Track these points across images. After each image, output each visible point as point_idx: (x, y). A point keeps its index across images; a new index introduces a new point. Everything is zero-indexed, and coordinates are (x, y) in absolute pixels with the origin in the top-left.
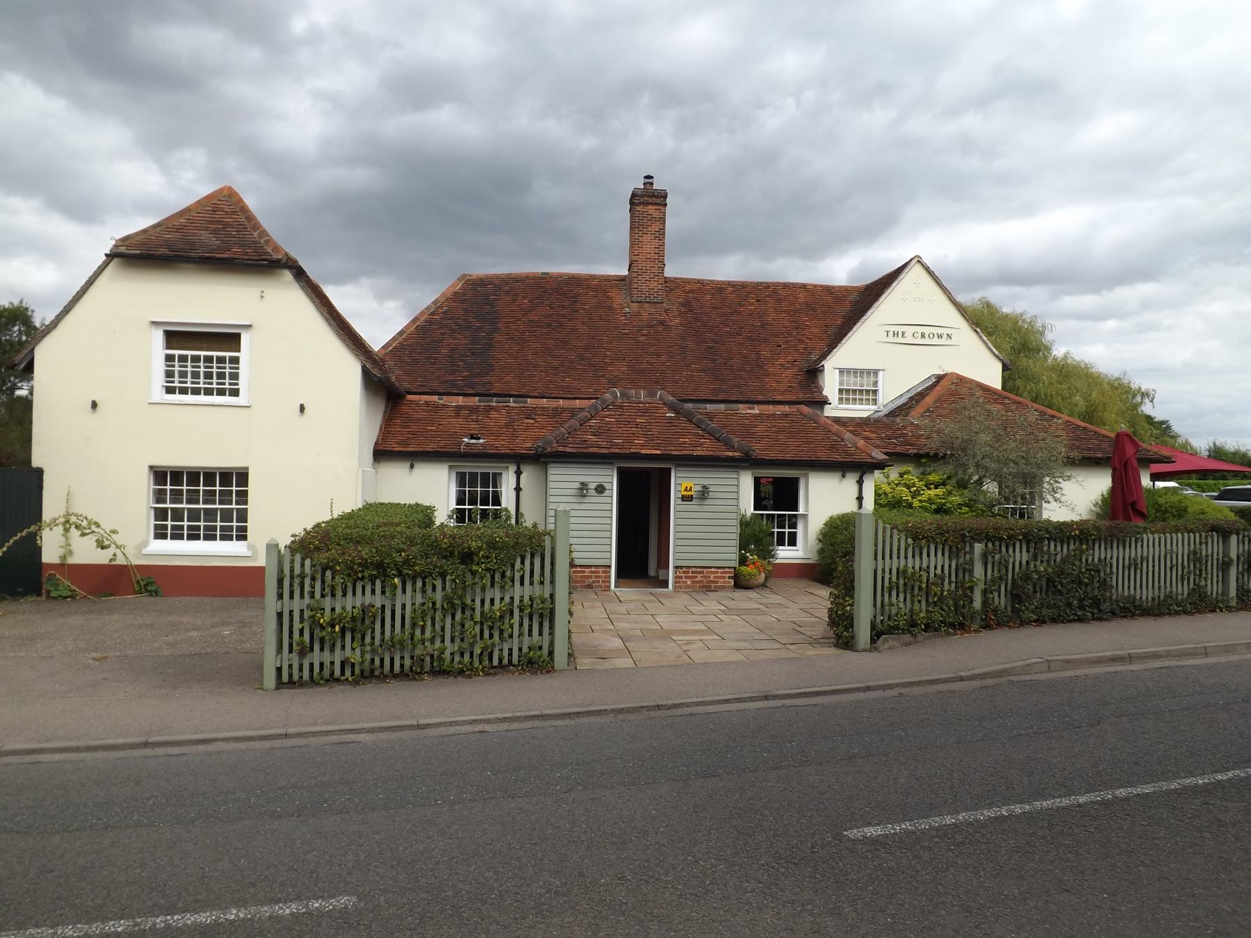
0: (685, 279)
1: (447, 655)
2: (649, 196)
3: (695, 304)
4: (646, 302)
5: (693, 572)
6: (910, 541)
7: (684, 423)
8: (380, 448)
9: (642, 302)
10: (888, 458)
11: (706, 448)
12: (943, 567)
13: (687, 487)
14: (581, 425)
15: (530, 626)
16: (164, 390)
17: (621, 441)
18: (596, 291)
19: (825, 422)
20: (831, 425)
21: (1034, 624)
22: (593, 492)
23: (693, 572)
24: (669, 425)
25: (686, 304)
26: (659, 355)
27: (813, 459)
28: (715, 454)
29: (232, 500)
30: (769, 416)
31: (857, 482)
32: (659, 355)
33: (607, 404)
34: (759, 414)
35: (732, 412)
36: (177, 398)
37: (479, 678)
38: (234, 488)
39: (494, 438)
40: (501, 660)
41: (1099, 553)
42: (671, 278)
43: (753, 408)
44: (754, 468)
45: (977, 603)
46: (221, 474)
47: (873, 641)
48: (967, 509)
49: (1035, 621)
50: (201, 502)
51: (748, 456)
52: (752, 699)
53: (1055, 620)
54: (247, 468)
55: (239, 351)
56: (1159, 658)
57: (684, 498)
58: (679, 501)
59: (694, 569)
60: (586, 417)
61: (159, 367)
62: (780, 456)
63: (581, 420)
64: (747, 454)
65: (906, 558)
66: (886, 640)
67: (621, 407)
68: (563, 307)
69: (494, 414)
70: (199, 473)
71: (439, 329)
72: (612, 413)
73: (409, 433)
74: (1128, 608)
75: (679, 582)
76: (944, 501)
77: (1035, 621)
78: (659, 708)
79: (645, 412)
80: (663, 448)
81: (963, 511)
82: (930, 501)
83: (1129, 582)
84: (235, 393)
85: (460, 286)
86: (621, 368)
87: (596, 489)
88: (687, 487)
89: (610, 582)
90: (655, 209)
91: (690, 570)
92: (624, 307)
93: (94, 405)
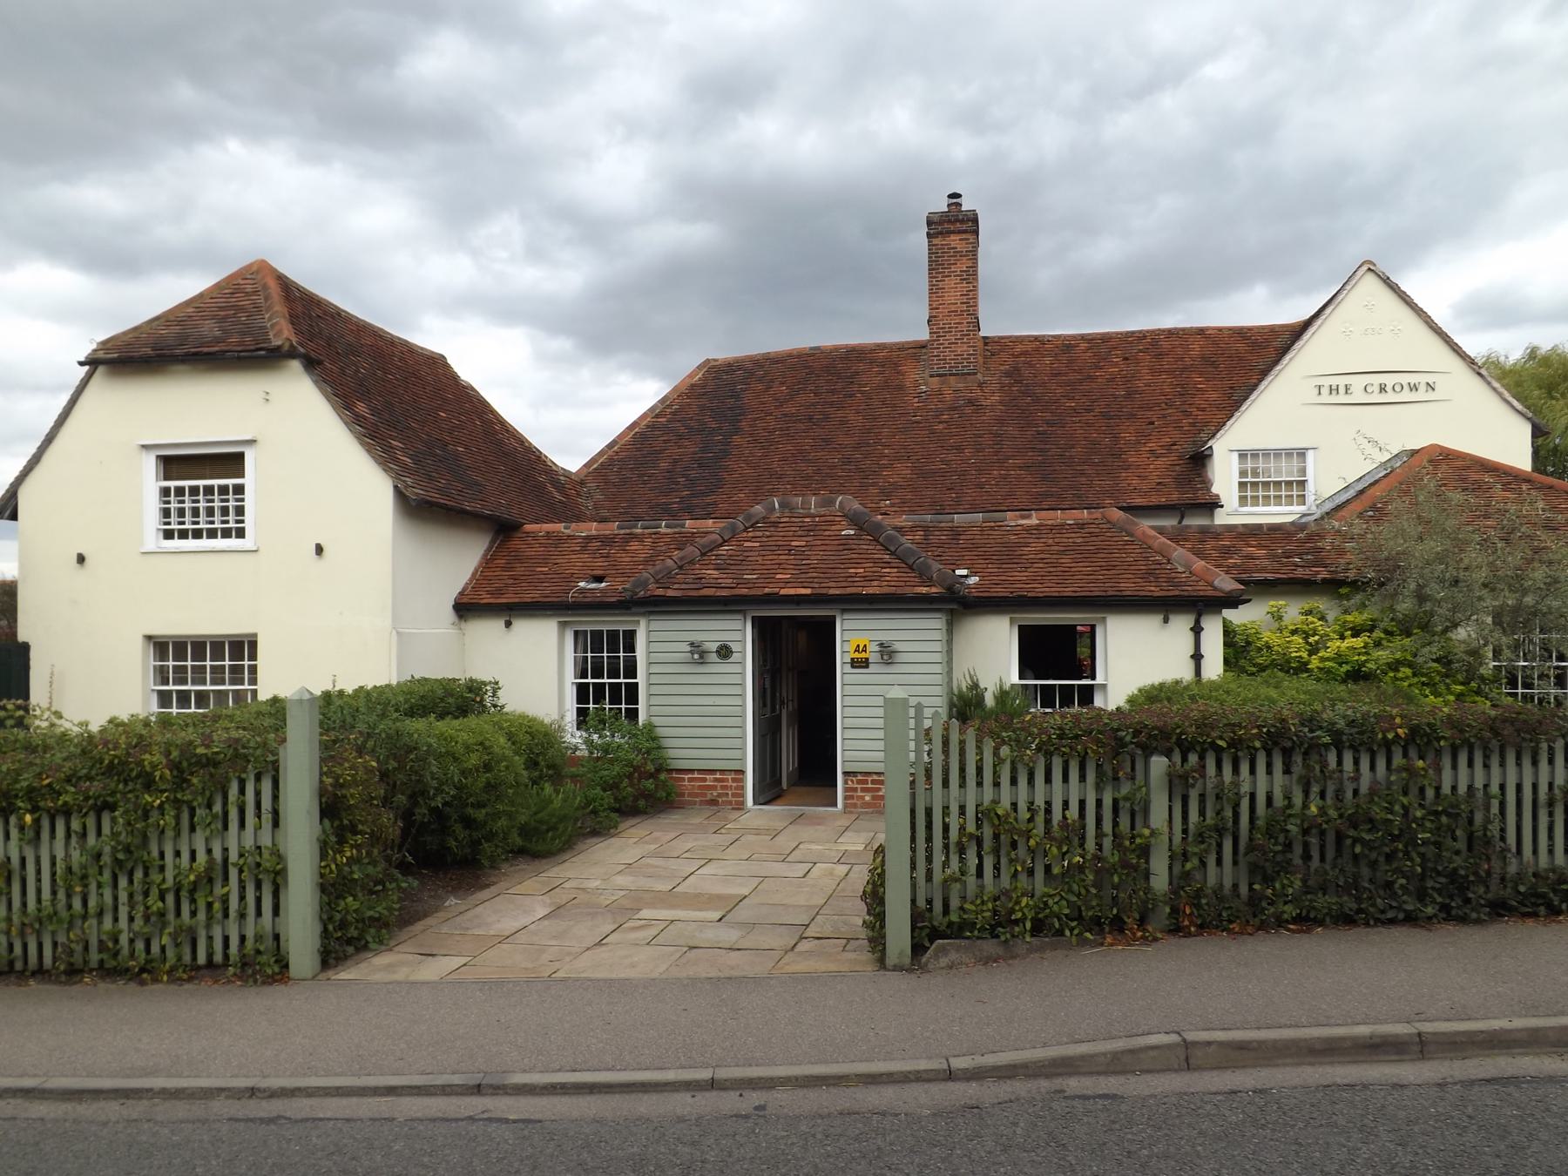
0: (1017, 337)
1: (124, 940)
2: (949, 222)
3: (1026, 372)
4: (951, 375)
5: (873, 782)
6: (1005, 751)
7: (866, 545)
8: (465, 600)
9: (946, 375)
10: (1243, 587)
11: (891, 580)
12: (1082, 803)
13: (858, 646)
14: (703, 554)
15: (259, 901)
16: (161, 535)
17: (755, 576)
18: (883, 366)
19: (1144, 533)
20: (1154, 537)
21: (1292, 927)
22: (714, 657)
23: (873, 782)
24: (841, 547)
25: (1014, 373)
26: (960, 449)
27: (1110, 593)
28: (899, 591)
29: (243, 679)
30: (1052, 528)
31: (1191, 629)
32: (960, 449)
33: (754, 521)
34: (1037, 525)
35: (993, 524)
36: (176, 544)
37: (160, 986)
38: (208, 663)
39: (622, 579)
40: (210, 955)
41: (1458, 777)
42: (994, 337)
43: (1029, 517)
44: (1014, 612)
45: (1160, 881)
46: (231, 643)
47: (918, 949)
48: (1408, 671)
49: (1295, 920)
50: (208, 682)
51: (954, 593)
52: (446, 1090)
53: (1346, 920)
54: (255, 635)
55: (243, 477)
56: (1508, 1047)
57: (855, 663)
58: (848, 668)
59: (875, 777)
60: (715, 541)
61: (153, 504)
62: (1054, 591)
63: (704, 546)
64: (950, 589)
65: (997, 784)
66: (943, 951)
67: (775, 524)
68: (833, 392)
69: (634, 545)
70: (186, 643)
71: (662, 435)
72: (760, 534)
73: (511, 577)
74: (1544, 896)
75: (852, 797)
76: (1363, 658)
77: (1295, 920)
78: (253, 1094)
79: (809, 530)
80: (817, 585)
81: (1400, 675)
82: (1340, 658)
83: (1551, 837)
84: (241, 533)
85: (700, 375)
86: (903, 470)
87: (717, 651)
88: (858, 646)
89: (743, 795)
90: (960, 240)
91: (870, 779)
92: (920, 385)
93: (81, 559)
